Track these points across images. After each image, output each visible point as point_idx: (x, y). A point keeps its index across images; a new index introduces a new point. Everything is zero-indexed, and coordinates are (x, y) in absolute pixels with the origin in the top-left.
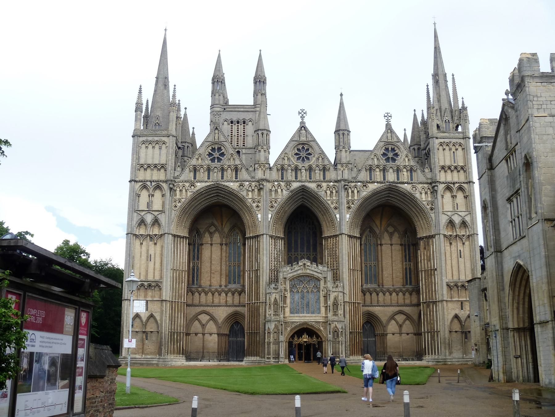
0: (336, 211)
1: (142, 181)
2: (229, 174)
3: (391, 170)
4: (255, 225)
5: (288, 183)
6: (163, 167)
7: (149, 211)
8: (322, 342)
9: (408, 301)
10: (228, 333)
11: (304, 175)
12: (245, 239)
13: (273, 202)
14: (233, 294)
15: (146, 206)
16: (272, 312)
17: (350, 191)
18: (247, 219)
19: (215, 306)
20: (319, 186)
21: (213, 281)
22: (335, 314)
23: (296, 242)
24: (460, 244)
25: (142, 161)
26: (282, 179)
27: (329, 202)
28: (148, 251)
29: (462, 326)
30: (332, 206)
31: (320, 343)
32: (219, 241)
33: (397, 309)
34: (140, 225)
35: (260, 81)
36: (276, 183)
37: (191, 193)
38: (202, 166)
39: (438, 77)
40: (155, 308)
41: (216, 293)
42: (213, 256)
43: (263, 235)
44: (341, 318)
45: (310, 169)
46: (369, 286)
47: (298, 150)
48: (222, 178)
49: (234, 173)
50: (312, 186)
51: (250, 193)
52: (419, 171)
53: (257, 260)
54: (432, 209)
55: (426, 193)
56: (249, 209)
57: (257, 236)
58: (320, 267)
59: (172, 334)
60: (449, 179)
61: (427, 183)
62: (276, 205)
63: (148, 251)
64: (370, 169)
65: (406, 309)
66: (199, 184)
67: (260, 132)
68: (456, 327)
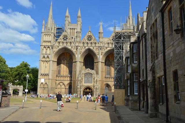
4: (75, 59)
5: (85, 47)
7: (46, 54)
11: (90, 45)
17: (102, 50)
22: (96, 84)
23: (88, 63)
25: (44, 40)
27: (96, 53)
31: (92, 92)
32: (66, 62)
34: (43, 58)
38: (61, 42)
44: (98, 85)
46: (108, 76)
47: (88, 38)
50: (92, 48)
53: (76, 68)
56: (74, 54)
58: (93, 71)
59: (52, 88)
64: (108, 43)
67: (78, 32)
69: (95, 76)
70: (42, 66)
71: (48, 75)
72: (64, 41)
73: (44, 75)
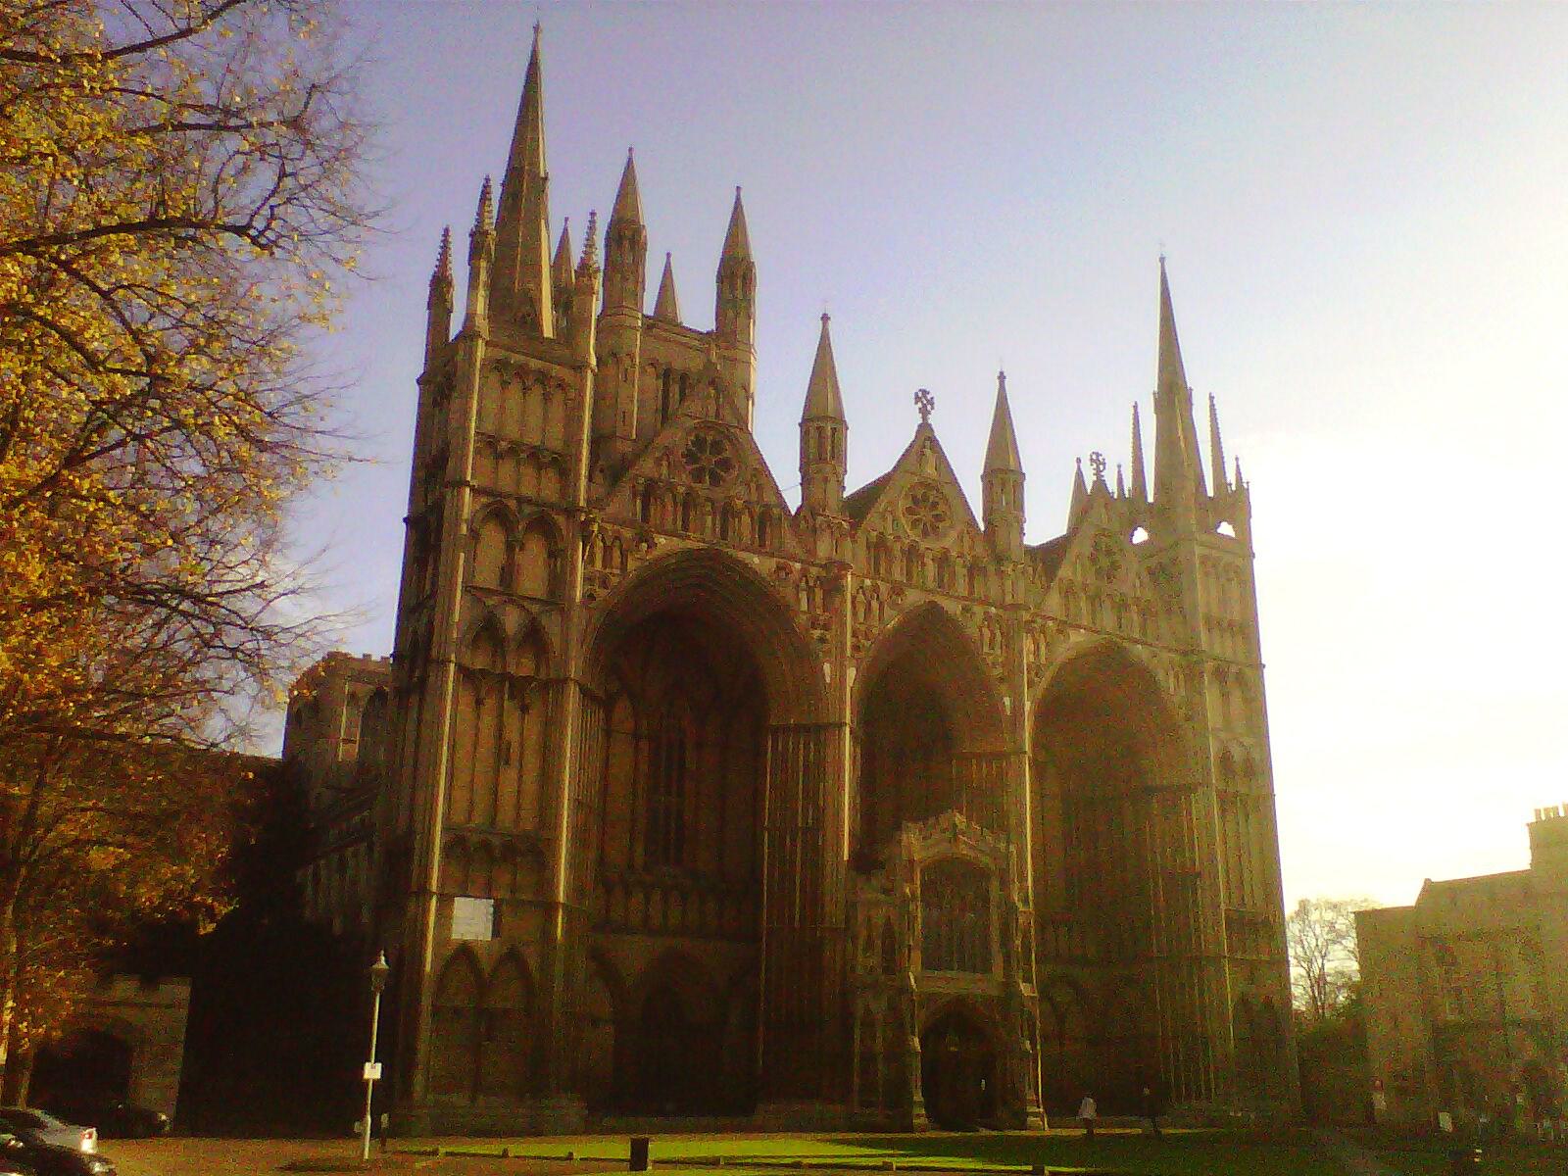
0: (1003, 688)
3: (1108, 603)
4: (811, 688)
5: (897, 590)
16: (874, 961)
20: (965, 609)
25: (489, 427)
26: (877, 571)
28: (500, 729)
30: (997, 672)
35: (735, 277)
36: (868, 582)
37: (638, 564)
39: (1172, 394)
45: (943, 560)
47: (914, 499)
50: (952, 607)
51: (803, 596)
53: (812, 794)
54: (1188, 719)
55: (1177, 677)
60: (1217, 651)
63: (500, 729)
66: (662, 540)
71: (536, 851)
72: (703, 489)
73: (486, 845)
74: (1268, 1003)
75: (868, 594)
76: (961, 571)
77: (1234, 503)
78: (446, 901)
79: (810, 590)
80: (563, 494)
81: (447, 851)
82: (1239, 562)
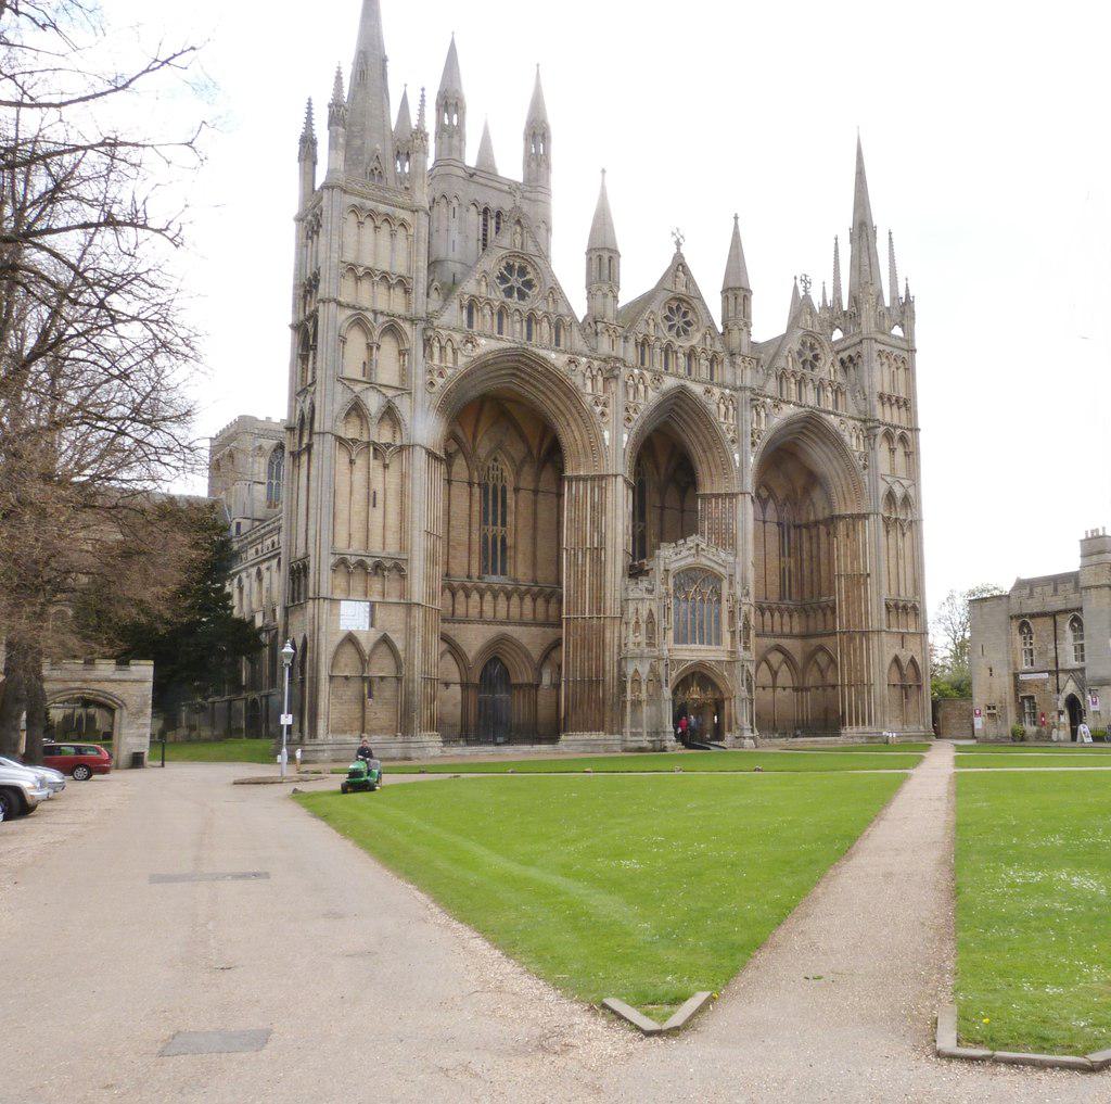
0: (735, 447)
1: (354, 307)
2: (544, 331)
3: (810, 385)
4: (594, 448)
5: (658, 378)
6: (404, 284)
8: (723, 701)
9: (786, 629)
10: (477, 682)
12: (560, 479)
13: (631, 411)
14: (495, 597)
15: (360, 370)
16: (642, 638)
18: (570, 437)
19: (460, 622)
20: (708, 391)
21: (452, 565)
22: (746, 648)
24: (900, 535)
25: (350, 257)
26: (643, 364)
27: (724, 427)
29: (902, 676)
30: (730, 436)
31: (718, 706)
32: (465, 475)
33: (772, 642)
34: (348, 414)
36: (636, 371)
38: (489, 302)
39: (863, 231)
40: (393, 621)
41: (461, 594)
42: (453, 509)
43: (616, 476)
45: (691, 355)
47: (671, 309)
48: (529, 338)
49: (553, 331)
50: (698, 389)
51: (589, 383)
52: (848, 395)
53: (597, 525)
54: (865, 468)
55: (858, 437)
56: (585, 418)
57: (602, 477)
58: (723, 555)
60: (888, 419)
61: (861, 420)
62: (636, 416)
65: (786, 643)
66: (483, 341)
68: (896, 679)
69: (739, 593)
70: (343, 489)
71: (399, 569)
73: (361, 564)
74: (913, 661)
75: (636, 381)
76: (705, 363)
77: (905, 310)
78: (334, 601)
79: (593, 378)
80: (408, 305)
81: (335, 568)
82: (905, 354)
